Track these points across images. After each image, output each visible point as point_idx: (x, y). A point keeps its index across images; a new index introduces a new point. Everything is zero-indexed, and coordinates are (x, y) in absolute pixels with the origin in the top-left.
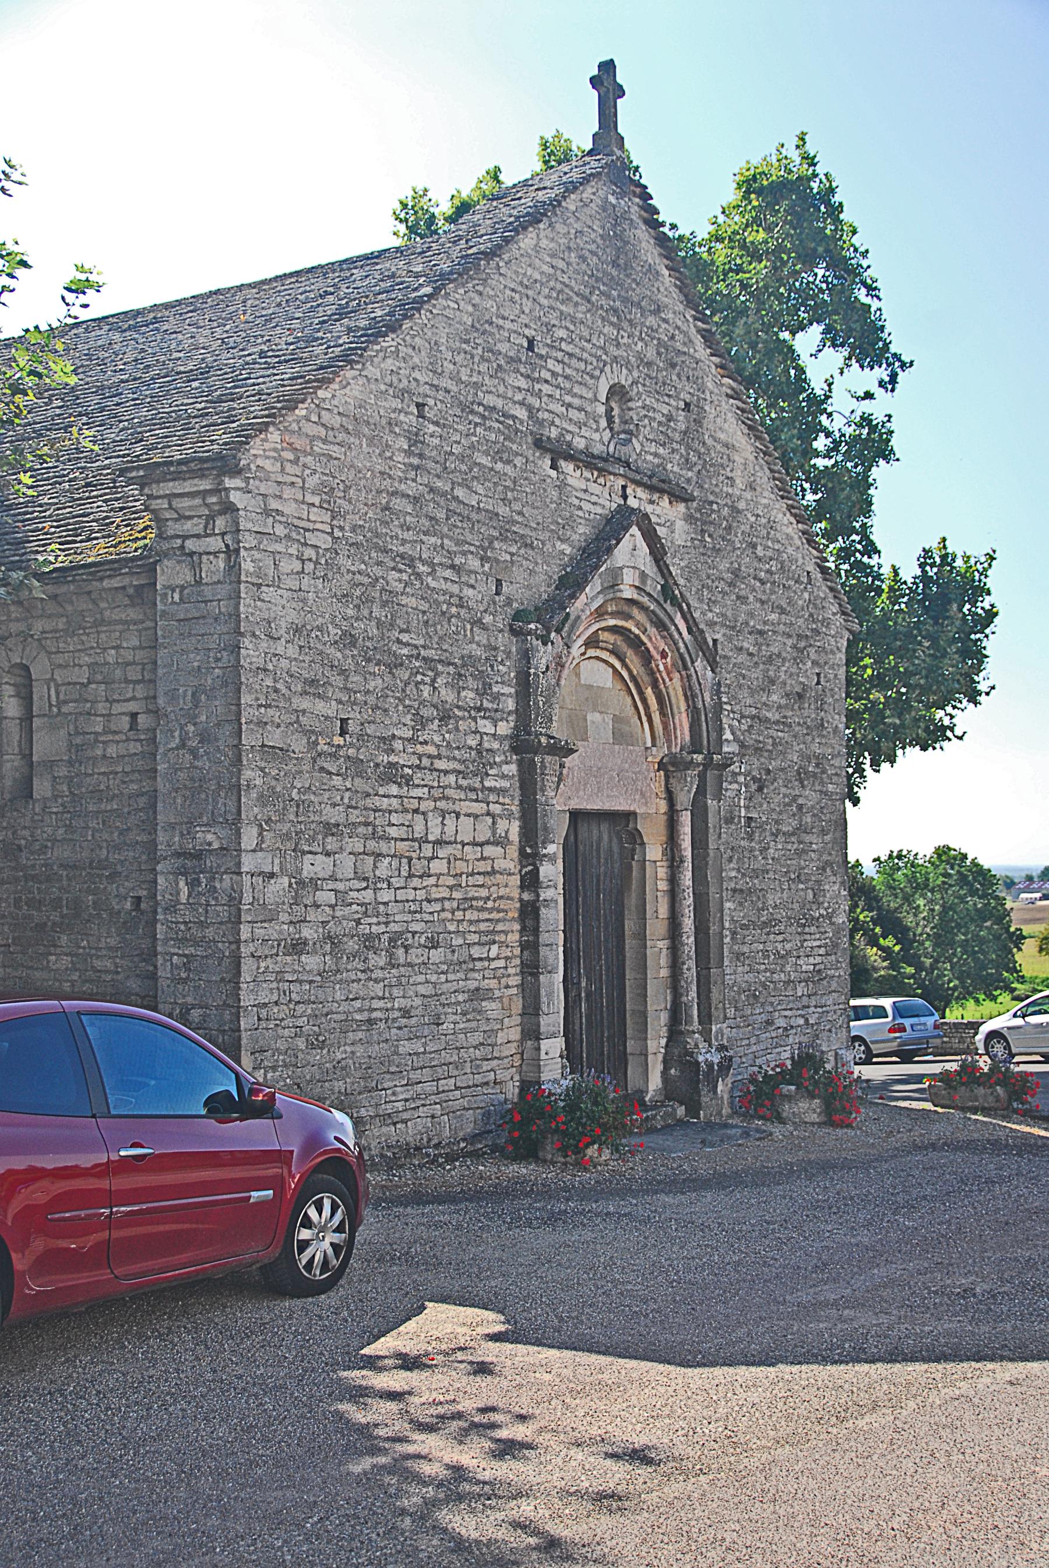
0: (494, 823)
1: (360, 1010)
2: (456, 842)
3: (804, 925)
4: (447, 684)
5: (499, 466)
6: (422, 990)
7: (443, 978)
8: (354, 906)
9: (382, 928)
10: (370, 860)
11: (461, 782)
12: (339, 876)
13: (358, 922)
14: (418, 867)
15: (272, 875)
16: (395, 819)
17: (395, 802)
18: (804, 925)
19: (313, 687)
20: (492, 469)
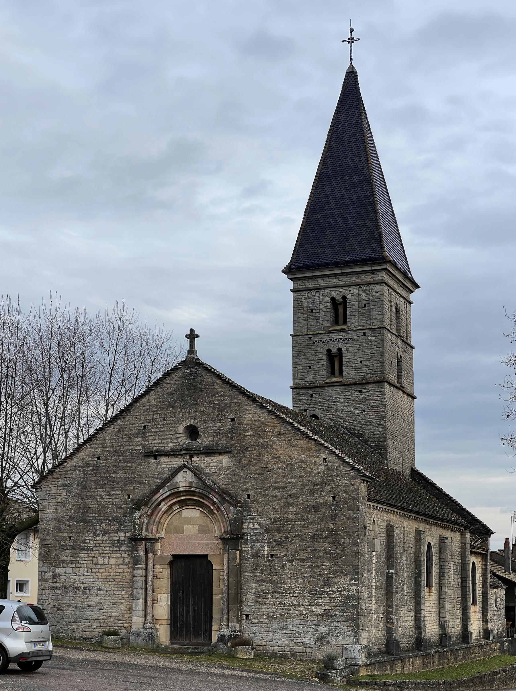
0: (124, 559)
1: (74, 604)
2: (108, 564)
3: (316, 594)
4: (106, 525)
5: (130, 465)
6: (95, 600)
7: (103, 598)
8: (72, 580)
9: (82, 585)
10: (78, 569)
11: (111, 549)
12: (67, 572)
13: (74, 583)
14: (93, 571)
15: (46, 572)
16: (86, 559)
17: (86, 555)
18: (316, 594)
19: (60, 530)
20: (127, 466)
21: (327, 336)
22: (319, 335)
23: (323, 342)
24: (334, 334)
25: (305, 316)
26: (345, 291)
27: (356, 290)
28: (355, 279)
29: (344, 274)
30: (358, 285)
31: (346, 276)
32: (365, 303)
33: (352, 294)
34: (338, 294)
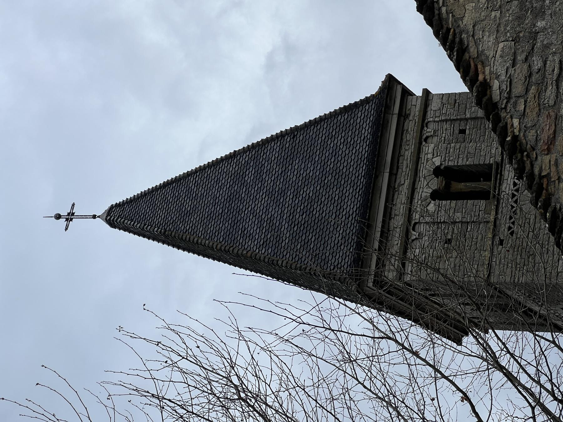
21: (503, 204)
22: (498, 223)
23: (515, 212)
24: (503, 189)
25: (455, 254)
26: (426, 169)
27: (428, 148)
28: (408, 153)
29: (395, 172)
30: (420, 143)
31: (400, 170)
32: (457, 131)
33: (435, 155)
34: (427, 185)
